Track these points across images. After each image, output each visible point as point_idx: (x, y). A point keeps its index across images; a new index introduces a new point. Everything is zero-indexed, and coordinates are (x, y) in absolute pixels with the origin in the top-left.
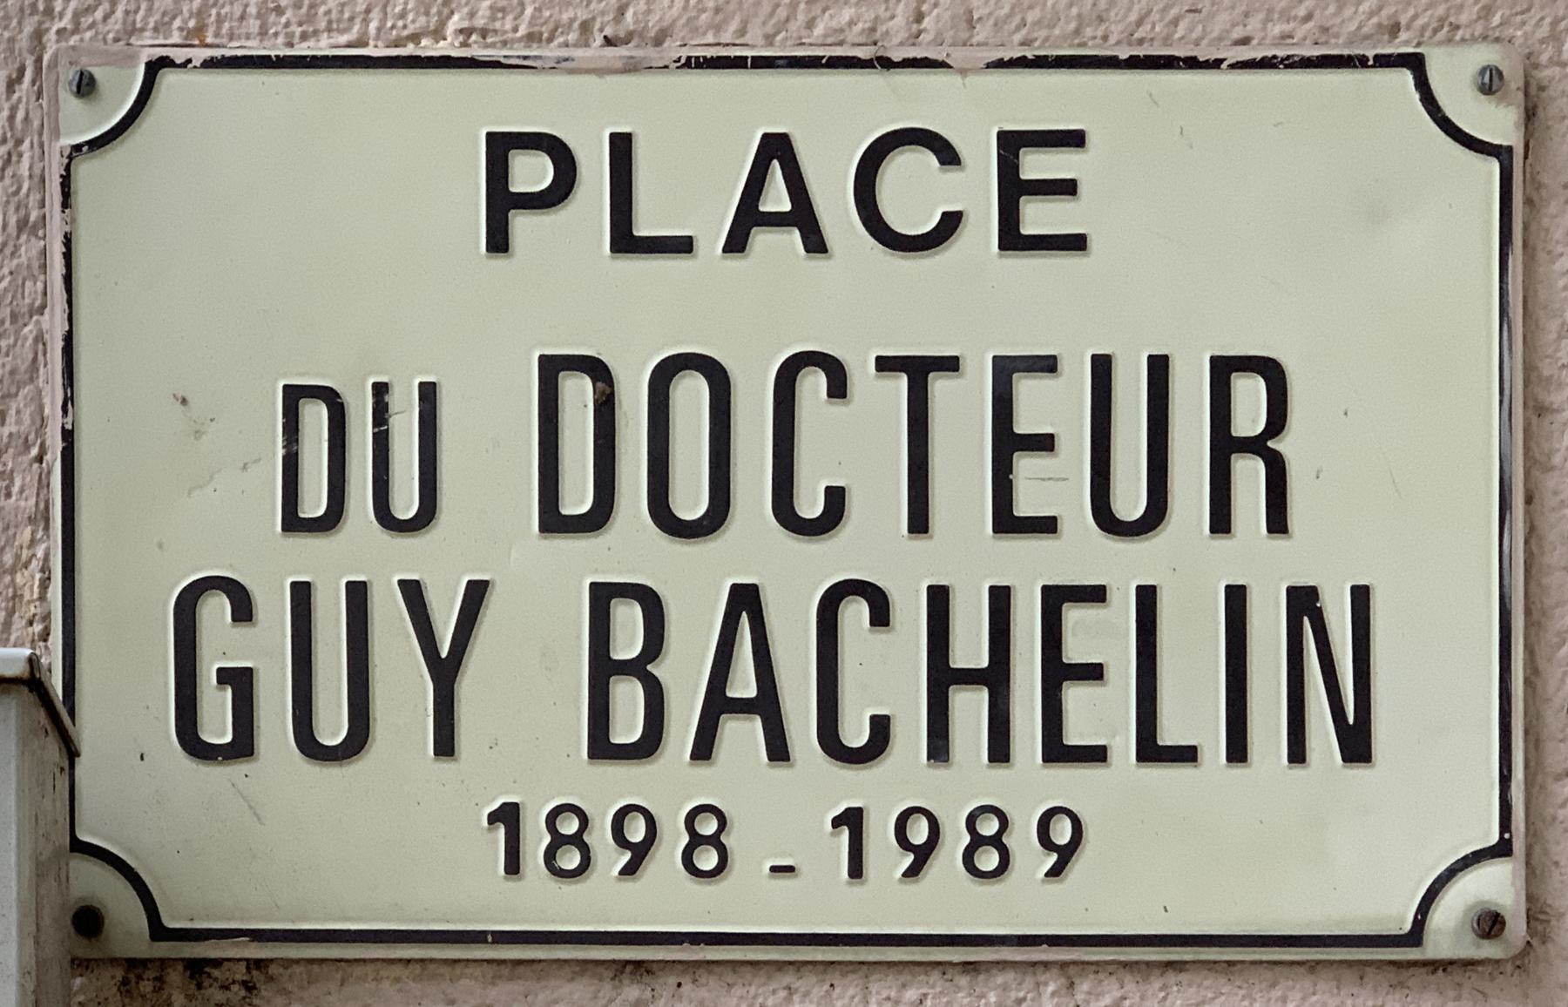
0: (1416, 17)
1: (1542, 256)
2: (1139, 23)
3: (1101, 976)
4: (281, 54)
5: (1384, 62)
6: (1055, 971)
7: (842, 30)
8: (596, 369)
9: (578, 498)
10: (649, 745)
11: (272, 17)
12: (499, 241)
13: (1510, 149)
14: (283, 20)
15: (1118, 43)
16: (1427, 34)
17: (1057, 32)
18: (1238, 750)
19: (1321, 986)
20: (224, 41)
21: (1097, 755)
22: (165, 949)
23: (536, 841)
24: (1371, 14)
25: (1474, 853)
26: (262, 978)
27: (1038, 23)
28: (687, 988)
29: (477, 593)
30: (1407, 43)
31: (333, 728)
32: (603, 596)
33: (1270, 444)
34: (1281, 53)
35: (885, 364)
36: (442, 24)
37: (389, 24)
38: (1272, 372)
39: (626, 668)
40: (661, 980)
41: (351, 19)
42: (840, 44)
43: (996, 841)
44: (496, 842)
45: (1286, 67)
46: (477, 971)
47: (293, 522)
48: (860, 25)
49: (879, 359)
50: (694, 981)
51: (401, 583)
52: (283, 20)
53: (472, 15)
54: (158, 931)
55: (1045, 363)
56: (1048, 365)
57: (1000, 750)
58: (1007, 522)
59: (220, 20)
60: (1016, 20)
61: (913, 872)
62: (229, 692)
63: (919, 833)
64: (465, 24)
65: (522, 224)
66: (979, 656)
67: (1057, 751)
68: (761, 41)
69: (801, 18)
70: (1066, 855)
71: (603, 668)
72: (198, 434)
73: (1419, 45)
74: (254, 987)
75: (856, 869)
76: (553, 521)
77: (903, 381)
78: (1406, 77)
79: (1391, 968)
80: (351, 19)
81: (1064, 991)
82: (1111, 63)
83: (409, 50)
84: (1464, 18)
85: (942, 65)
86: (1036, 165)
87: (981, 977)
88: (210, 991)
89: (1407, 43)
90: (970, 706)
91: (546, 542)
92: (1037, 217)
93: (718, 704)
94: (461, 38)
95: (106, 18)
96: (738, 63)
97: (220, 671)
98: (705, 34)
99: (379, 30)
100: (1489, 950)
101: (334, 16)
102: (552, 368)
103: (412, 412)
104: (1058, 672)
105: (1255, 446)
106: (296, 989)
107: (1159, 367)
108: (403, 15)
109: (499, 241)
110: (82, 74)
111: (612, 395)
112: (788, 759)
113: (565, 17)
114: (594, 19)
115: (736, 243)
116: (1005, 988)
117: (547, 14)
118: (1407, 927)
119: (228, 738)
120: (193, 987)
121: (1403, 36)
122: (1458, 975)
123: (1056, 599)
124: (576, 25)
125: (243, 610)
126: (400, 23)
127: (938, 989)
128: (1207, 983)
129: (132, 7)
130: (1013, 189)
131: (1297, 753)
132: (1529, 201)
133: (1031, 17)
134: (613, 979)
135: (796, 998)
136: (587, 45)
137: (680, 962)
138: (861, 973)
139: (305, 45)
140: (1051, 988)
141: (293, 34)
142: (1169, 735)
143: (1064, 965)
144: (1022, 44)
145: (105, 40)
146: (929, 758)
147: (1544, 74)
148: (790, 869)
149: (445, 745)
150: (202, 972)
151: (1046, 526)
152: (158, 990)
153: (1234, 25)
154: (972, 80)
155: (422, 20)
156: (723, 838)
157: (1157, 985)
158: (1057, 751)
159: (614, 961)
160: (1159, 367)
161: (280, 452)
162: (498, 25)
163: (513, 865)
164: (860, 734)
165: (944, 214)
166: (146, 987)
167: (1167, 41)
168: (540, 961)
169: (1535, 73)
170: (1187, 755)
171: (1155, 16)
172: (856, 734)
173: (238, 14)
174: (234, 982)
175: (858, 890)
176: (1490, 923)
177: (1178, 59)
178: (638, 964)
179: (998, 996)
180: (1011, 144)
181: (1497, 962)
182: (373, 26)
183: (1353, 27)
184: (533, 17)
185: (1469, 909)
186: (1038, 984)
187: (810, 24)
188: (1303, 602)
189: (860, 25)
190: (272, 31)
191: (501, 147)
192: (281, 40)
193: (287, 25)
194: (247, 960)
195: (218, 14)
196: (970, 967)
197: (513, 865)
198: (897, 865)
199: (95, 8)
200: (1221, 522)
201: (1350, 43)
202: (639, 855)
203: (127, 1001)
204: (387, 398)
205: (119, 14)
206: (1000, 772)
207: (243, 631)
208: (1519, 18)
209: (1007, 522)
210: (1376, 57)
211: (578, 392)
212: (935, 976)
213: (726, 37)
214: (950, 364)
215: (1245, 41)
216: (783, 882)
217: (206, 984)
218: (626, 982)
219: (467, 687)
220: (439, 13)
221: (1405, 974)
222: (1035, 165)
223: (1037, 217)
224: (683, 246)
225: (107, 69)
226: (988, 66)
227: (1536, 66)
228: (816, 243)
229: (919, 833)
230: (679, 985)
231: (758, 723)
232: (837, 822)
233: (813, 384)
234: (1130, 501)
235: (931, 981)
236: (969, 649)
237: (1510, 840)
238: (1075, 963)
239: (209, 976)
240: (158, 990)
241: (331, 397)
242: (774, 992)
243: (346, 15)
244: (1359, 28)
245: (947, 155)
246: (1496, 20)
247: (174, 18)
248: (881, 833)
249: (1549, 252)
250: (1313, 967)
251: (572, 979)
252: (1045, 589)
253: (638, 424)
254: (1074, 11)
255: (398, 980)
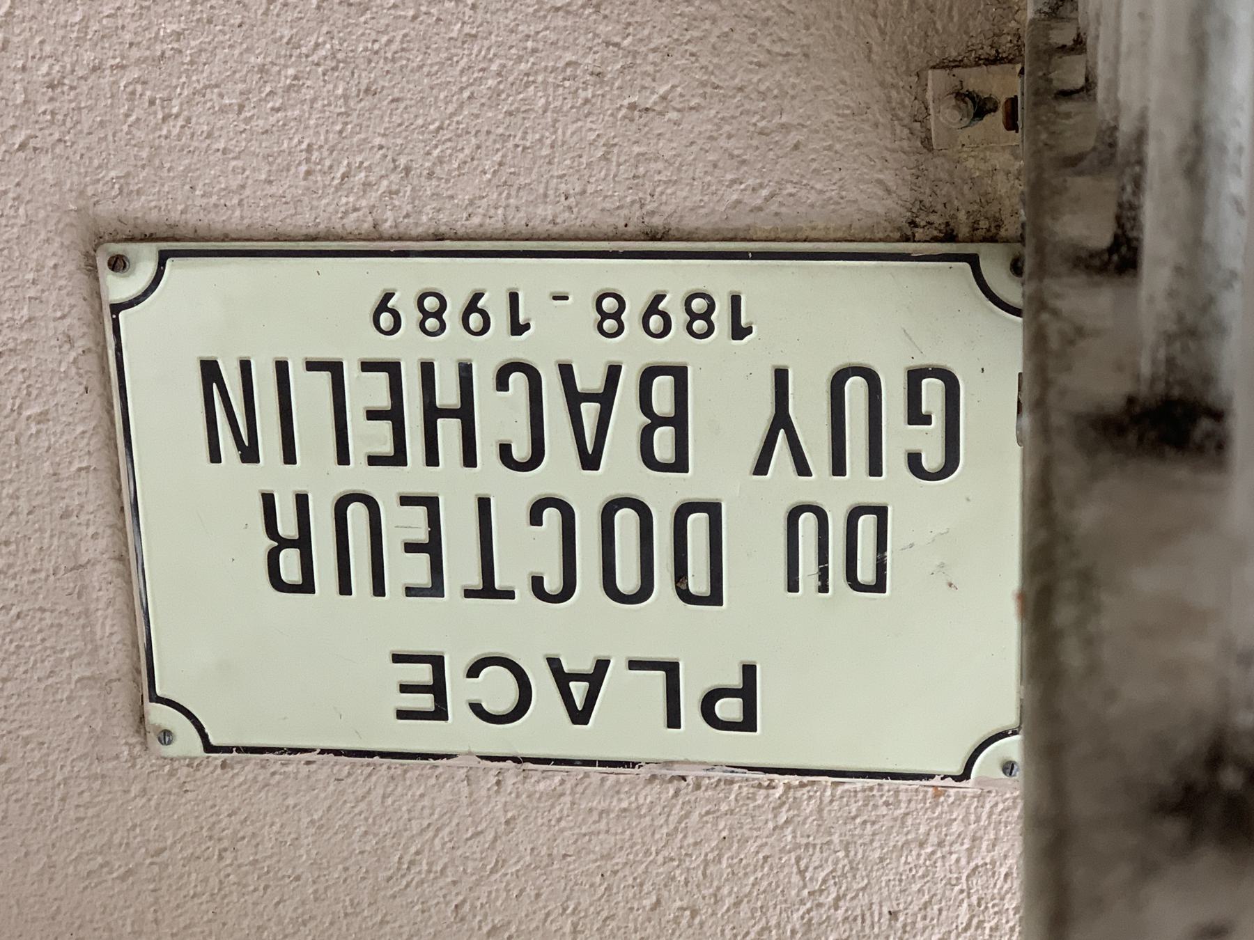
0: (212, 772)
1: (128, 642)
2: (370, 775)
3: (356, 232)
4: (884, 780)
5: (228, 749)
6: (386, 235)
7: (544, 778)
8: (686, 596)
9: (697, 524)
10: (649, 374)
11: (891, 800)
12: (749, 672)
13: (151, 701)
14: (884, 799)
15: (381, 765)
16: (205, 762)
17: (417, 772)
18: (282, 368)
19: (219, 226)
20: (921, 789)
21: (367, 366)
22: (970, 248)
23: (721, 317)
24: (237, 774)
25: (133, 306)
26: (905, 230)
27: (429, 777)
28: (621, 224)
29: (761, 467)
30: (216, 759)
31: (855, 388)
32: (680, 464)
33: (276, 544)
34: (286, 756)
35: (509, 594)
36: (786, 792)
37: (818, 794)
38: (277, 582)
39: (664, 421)
40: (638, 228)
41: (842, 797)
42: (544, 771)
43: (426, 315)
44: (747, 317)
45: (282, 749)
46: (760, 234)
47: (881, 512)
48: (533, 780)
49: (513, 598)
50: (616, 228)
51: (811, 475)
52: (884, 799)
53: (767, 796)
54: (973, 261)
55: (413, 592)
56: (411, 591)
57: (427, 370)
58: (431, 504)
59: (924, 800)
60: (442, 779)
61: (478, 296)
62: (924, 410)
63: (475, 320)
64: (771, 791)
65: (736, 681)
66: (443, 426)
67: (392, 369)
68: (591, 774)
69: (568, 786)
70: (382, 306)
71: (679, 421)
72: (942, 566)
73: (208, 757)
74: (910, 223)
75: (514, 298)
76: (713, 510)
77: (498, 585)
78: (214, 741)
79: (178, 237)
80: (842, 797)
81: (380, 222)
82: (384, 755)
83: (806, 779)
84: (185, 770)
85: (482, 757)
86: (426, 702)
87: (432, 231)
88: (941, 221)
89: (216, 759)
90: (448, 395)
91: (718, 497)
92: (423, 673)
93: (606, 399)
94: (774, 784)
95: (996, 804)
96: (603, 763)
97: (930, 423)
98: (626, 780)
99: (824, 791)
100: (117, 248)
101: (853, 800)
102: (715, 598)
103: (803, 576)
104: (395, 415)
105: (284, 543)
106: (882, 222)
107: (345, 588)
108: (810, 798)
109: (749, 672)
110: (1011, 774)
111: (676, 582)
112: (560, 365)
113: (710, 793)
114: (693, 791)
115: (602, 666)
116: (416, 224)
117: (721, 795)
118: (169, 262)
119: (925, 382)
120: (952, 224)
121: (219, 762)
122: (137, 233)
123: (398, 458)
124: (703, 788)
125: (914, 462)
126: (811, 794)
127: (459, 223)
128: (290, 228)
129: (980, 810)
130: (438, 688)
131: (245, 366)
132: (139, 672)
133: (433, 781)
134: (670, 229)
135: (550, 218)
136: (697, 777)
137: (625, 240)
138: (508, 233)
139: (871, 785)
140: (388, 224)
141: (879, 791)
142: (325, 377)
143: (381, 238)
144: (437, 767)
145: (997, 792)
146: (471, 365)
147: (139, 739)
148: (555, 298)
149: (781, 377)
150: (946, 234)
151: (406, 501)
152: (976, 222)
153: (315, 771)
154: (466, 749)
155: (799, 794)
156: (599, 317)
157: (322, 226)
158: (392, 369)
159: (669, 240)
160: (345, 588)
161: (888, 553)
162: (751, 790)
163: (736, 301)
164: (515, 380)
165: (477, 677)
166: (984, 224)
167: (354, 765)
168: (717, 240)
169: (143, 740)
170: (312, 366)
171: (361, 778)
172: (518, 380)
173: (913, 803)
174: (924, 227)
175: (512, 285)
176: (118, 264)
177: (345, 755)
178: (653, 238)
179: (420, 219)
180: (440, 713)
181: (114, 241)
182: (828, 793)
183: (247, 768)
184: (730, 793)
185: (133, 273)
186: (396, 227)
187: (562, 782)
188: (249, 454)
189: (533, 780)
190: (891, 793)
191: (748, 723)
192: (886, 788)
193: (882, 796)
194: (914, 241)
195: (925, 803)
196: (439, 237)
197: (736, 301)
198: (488, 300)
199: (1002, 810)
200: (302, 501)
201: (248, 760)
202: (653, 307)
203: (997, 215)
204: (820, 583)
205: (988, 806)
206: (427, 357)
207: (914, 447)
208: (154, 769)
209: (431, 504)
210: (232, 752)
211: (698, 582)
212: (461, 231)
213: (612, 778)
214: (469, 593)
215: (308, 763)
216: (560, 290)
217: (942, 227)
218: (660, 228)
219: (767, 411)
220: (788, 798)
221: (170, 234)
222: (426, 702)
223: (423, 673)
224: (634, 665)
225: (994, 777)
226: (455, 756)
227: (142, 744)
228: (554, 664)
229: (475, 320)
230: (626, 226)
231: (579, 388)
232: (527, 327)
233: (553, 584)
234: (357, 515)
235: (463, 229)
236: (449, 430)
237: (112, 314)
238: (374, 240)
239: (940, 231)
240: (976, 222)
241: (855, 585)
242: (564, 221)
243: (845, 799)
244: (244, 767)
245: (477, 709)
246: (167, 768)
247: (953, 803)
248: (500, 320)
249: (124, 644)
250: (226, 238)
251: (697, 229)
252: (405, 464)
253: (660, 564)
254: (408, 783)
255: (814, 228)
